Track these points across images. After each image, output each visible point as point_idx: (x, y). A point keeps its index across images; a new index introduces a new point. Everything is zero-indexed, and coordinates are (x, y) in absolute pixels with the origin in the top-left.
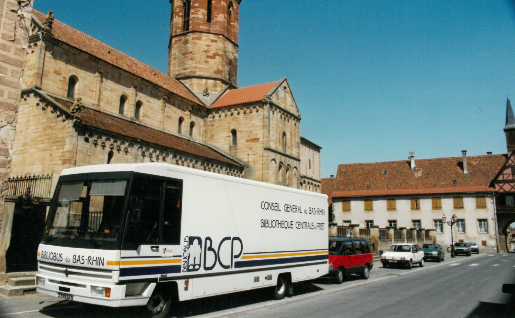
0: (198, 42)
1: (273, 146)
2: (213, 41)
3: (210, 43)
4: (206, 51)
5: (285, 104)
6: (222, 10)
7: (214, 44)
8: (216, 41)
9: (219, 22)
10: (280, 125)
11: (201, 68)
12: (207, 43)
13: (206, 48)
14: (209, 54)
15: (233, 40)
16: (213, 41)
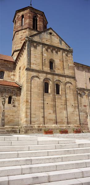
0: (17, 35)
1: (33, 67)
2: (24, 33)
3: (22, 34)
4: (21, 38)
5: (52, 42)
6: (28, 18)
7: (25, 33)
8: (25, 32)
9: (27, 23)
10: (45, 55)
11: (19, 46)
12: (21, 35)
13: (20, 37)
14: (22, 39)
15: (39, 30)
16: (24, 33)
